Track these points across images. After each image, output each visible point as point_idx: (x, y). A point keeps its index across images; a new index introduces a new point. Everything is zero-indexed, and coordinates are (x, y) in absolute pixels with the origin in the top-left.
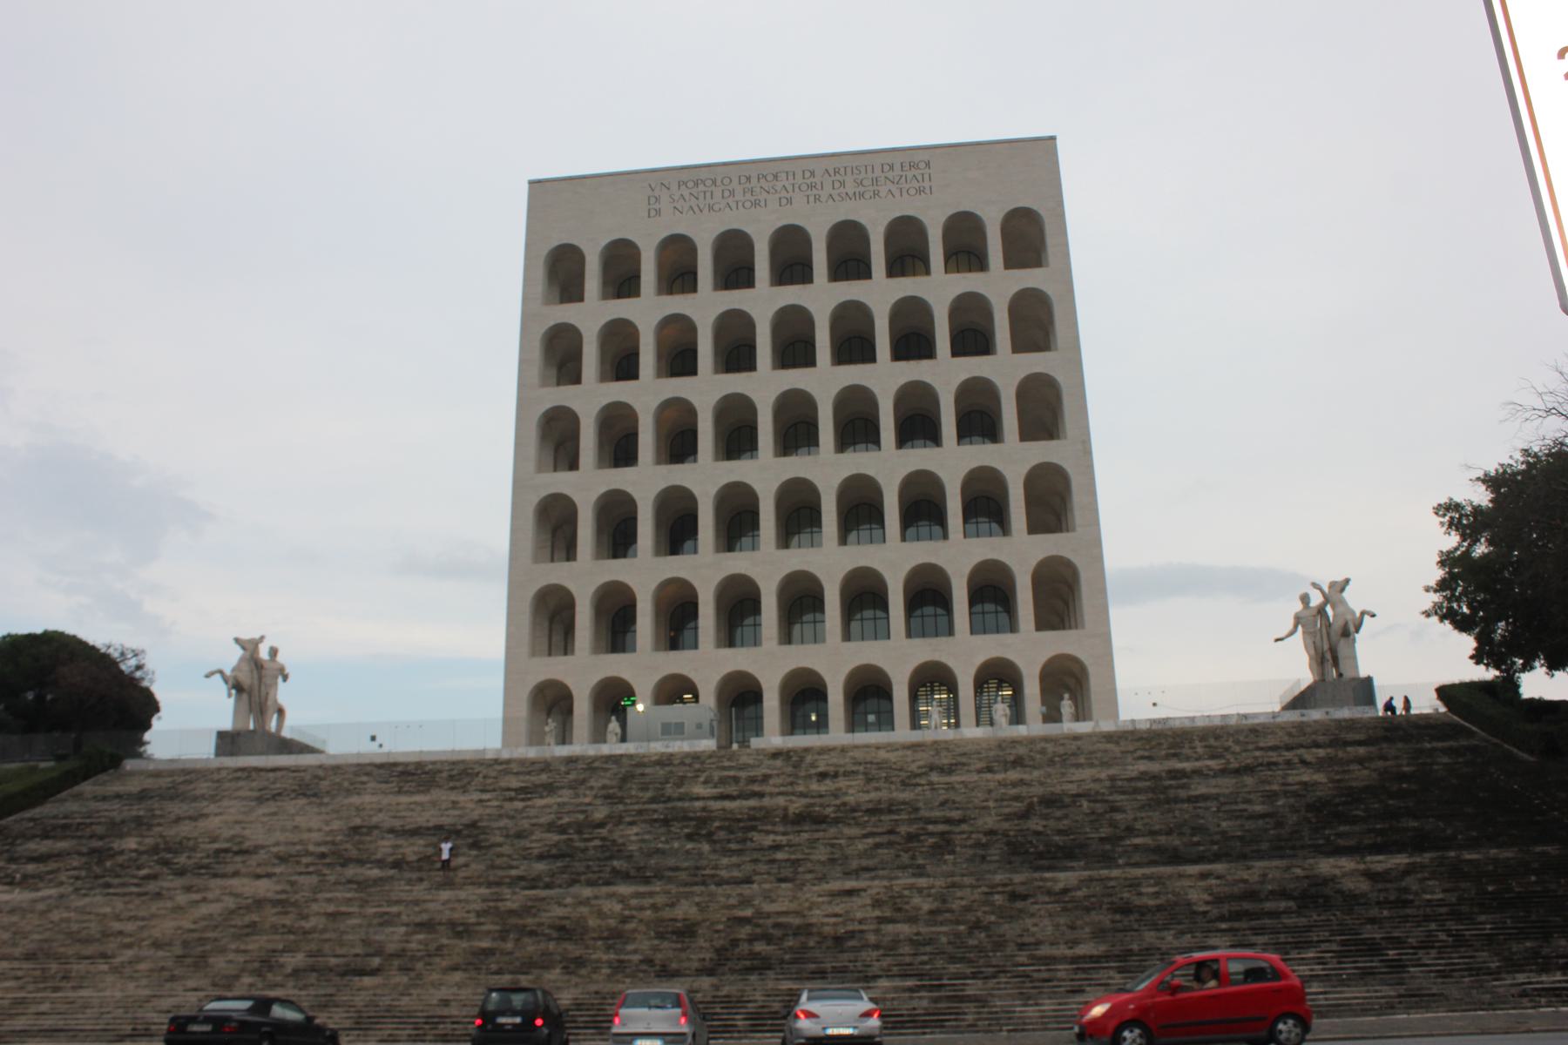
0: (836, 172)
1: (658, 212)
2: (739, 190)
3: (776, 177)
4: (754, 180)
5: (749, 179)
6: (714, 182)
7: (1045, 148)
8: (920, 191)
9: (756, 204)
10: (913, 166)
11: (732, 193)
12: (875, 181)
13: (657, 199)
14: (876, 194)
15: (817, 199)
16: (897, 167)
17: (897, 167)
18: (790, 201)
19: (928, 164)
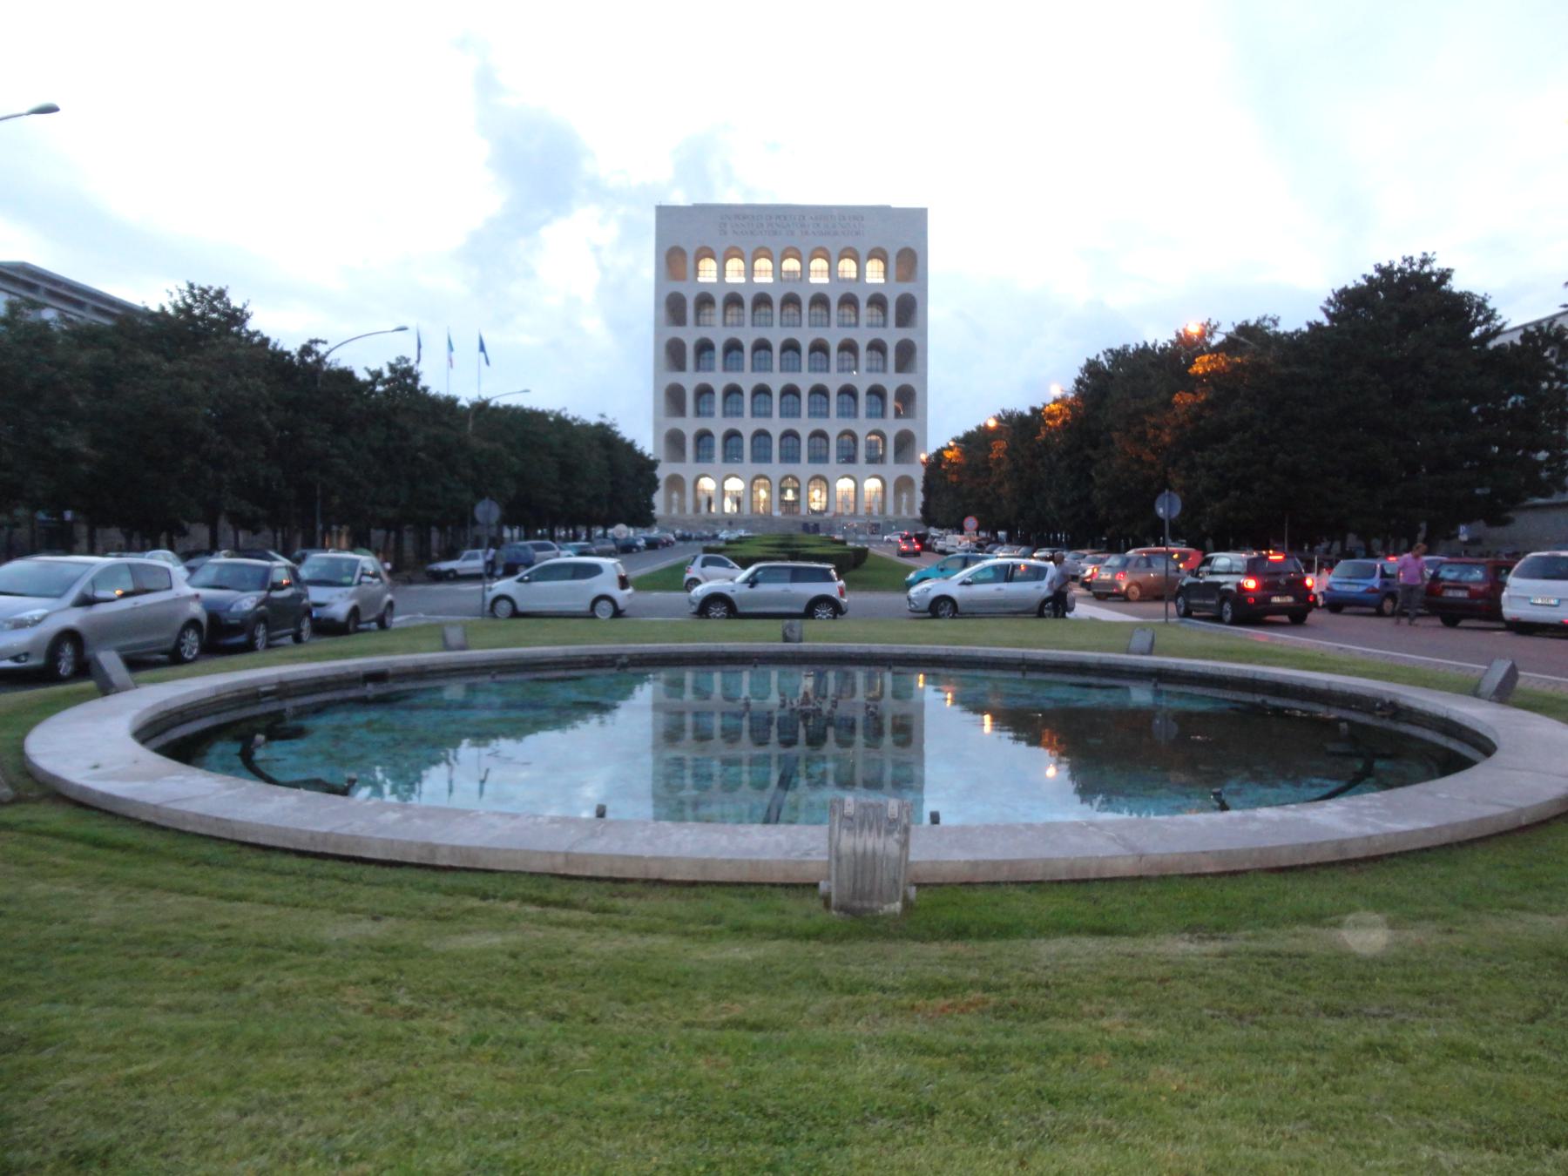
1: (725, 233)
8: (857, 233)
9: (775, 233)
10: (855, 218)
12: (834, 226)
13: (725, 225)
15: (807, 233)
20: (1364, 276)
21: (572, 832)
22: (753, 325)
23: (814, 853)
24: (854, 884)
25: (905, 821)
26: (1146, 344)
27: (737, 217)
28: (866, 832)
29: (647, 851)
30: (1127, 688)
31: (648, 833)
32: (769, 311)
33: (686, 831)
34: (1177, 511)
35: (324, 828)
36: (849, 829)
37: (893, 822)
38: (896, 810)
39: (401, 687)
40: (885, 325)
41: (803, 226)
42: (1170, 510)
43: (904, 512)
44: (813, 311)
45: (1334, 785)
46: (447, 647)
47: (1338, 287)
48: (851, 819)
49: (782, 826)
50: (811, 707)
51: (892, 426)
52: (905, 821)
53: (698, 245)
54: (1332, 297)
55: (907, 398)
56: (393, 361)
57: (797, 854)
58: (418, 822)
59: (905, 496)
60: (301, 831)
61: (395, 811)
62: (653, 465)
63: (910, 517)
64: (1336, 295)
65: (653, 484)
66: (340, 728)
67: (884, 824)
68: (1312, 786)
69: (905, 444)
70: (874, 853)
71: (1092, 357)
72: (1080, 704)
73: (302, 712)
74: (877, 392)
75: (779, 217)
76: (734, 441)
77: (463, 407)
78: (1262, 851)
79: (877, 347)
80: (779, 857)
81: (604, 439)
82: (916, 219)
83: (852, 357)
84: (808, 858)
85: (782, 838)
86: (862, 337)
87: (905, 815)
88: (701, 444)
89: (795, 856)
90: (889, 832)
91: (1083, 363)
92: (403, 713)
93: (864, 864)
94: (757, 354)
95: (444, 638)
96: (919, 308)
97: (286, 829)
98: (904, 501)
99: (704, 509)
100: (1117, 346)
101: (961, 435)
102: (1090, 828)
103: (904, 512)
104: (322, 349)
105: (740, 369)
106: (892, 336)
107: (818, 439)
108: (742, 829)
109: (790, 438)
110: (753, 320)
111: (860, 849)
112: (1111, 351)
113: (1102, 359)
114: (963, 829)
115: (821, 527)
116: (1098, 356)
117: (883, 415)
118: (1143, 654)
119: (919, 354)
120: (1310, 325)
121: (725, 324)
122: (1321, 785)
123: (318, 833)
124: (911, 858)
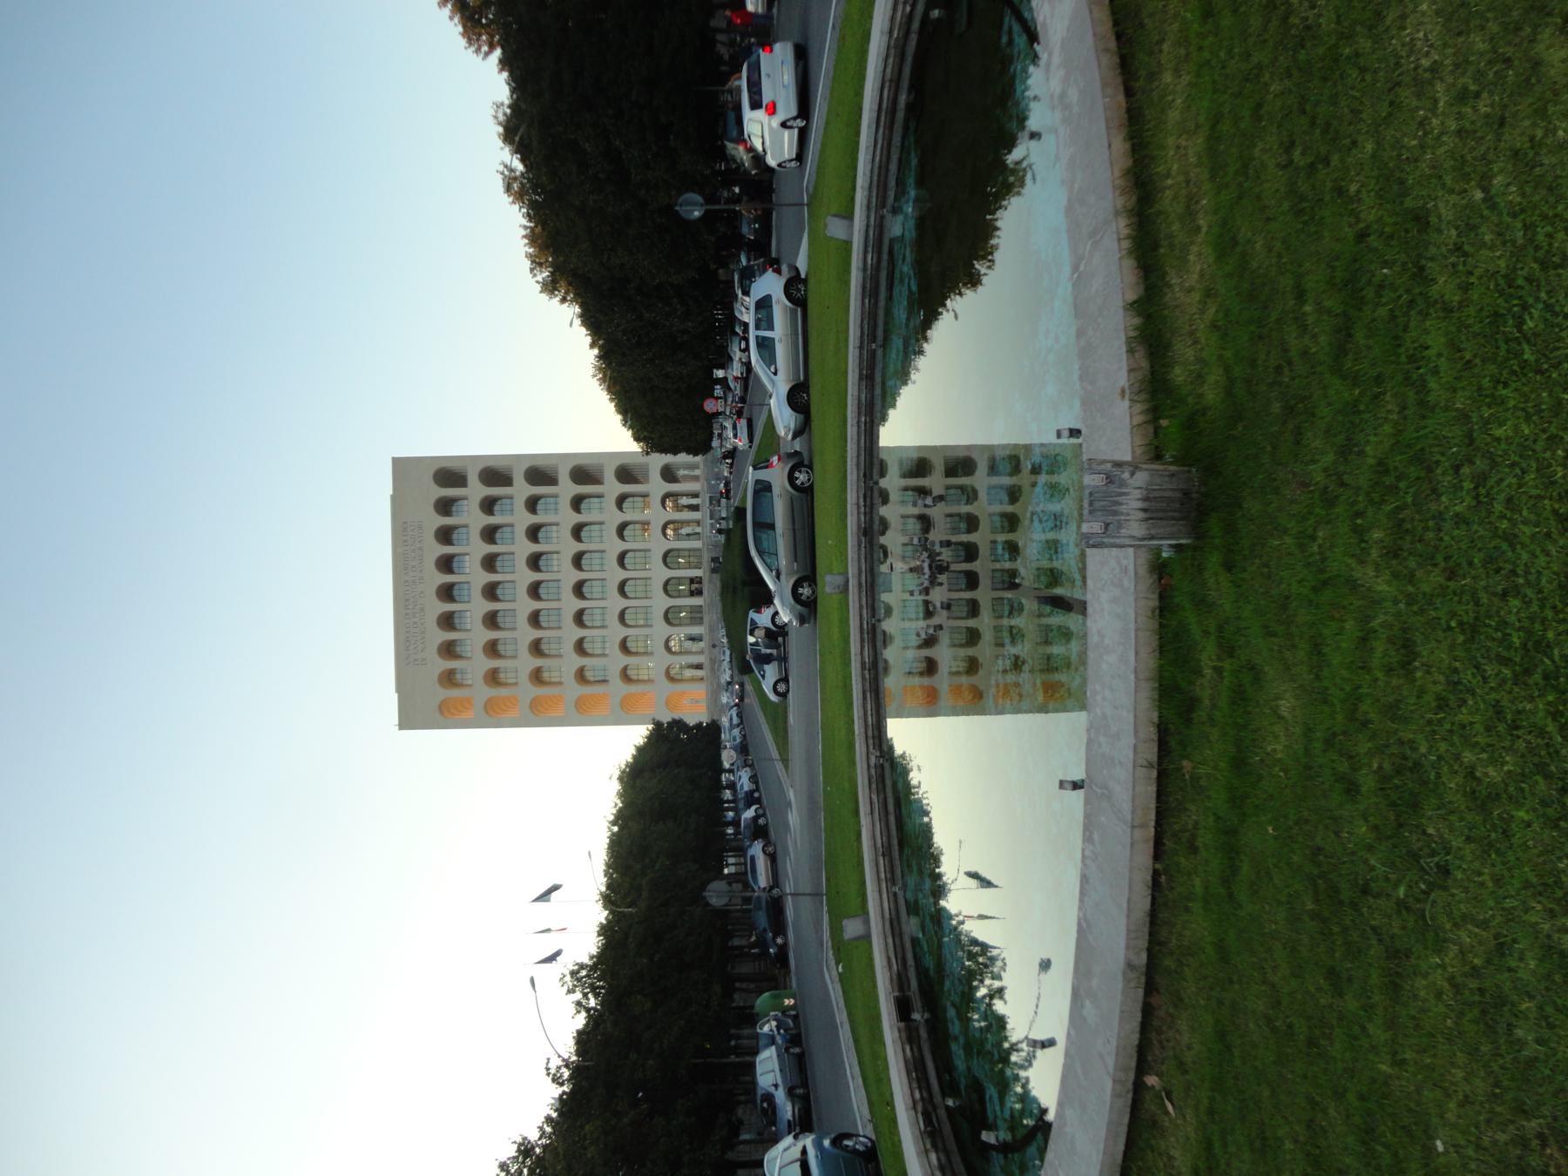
0: (406, 569)
1: (424, 660)
2: (415, 620)
3: (407, 600)
4: (408, 611)
6: (407, 632)
7: (402, 468)
8: (420, 527)
9: (422, 610)
10: (405, 530)
11: (415, 623)
13: (416, 660)
14: (420, 549)
15: (421, 578)
16: (405, 538)
17: (405, 538)
18: (422, 592)
20: (451, 18)
21: (1103, 819)
22: (514, 629)
23: (1124, 562)
24: (1173, 519)
25: (1109, 466)
26: (525, 237)
28: (1123, 508)
29: (1128, 740)
30: (892, 241)
31: (1102, 739)
33: (1099, 698)
34: (699, 198)
35: (1109, 1085)
36: (1120, 526)
37: (1110, 479)
38: (1093, 476)
39: (914, 983)
40: (511, 498)
41: (414, 582)
42: (694, 204)
43: (697, 472)
44: (499, 569)
45: (1008, 20)
46: (866, 937)
47: (463, 42)
48: (1107, 525)
49: (1089, 597)
50: (926, 565)
51: (613, 487)
52: (1109, 466)
54: (473, 49)
55: (585, 473)
56: (565, 989)
57: (1126, 583)
58: (1094, 983)
60: (1111, 1107)
61: (1082, 1006)
62: (658, 725)
63: (701, 466)
64: (470, 44)
65: (678, 724)
66: (968, 1048)
67: (1112, 488)
68: (1011, 42)
69: (626, 474)
70: (1146, 499)
71: (539, 287)
72: (914, 288)
73: (950, 1088)
76: (630, 645)
77: (606, 919)
78: (1104, 85)
79: (532, 504)
80: (1132, 598)
81: (636, 777)
82: (402, 468)
83: (543, 529)
84: (1131, 567)
85: (1104, 597)
86: (524, 519)
87: (1103, 467)
88: (635, 678)
89: (1129, 583)
90: (1123, 484)
91: (544, 297)
92: (947, 984)
93: (1155, 510)
94: (543, 624)
95: (858, 938)
96: (490, 464)
97: (1110, 1123)
98: (686, 472)
99: (699, 673)
100: (527, 264)
101: (619, 417)
102: (1082, 268)
103: (697, 472)
104: (555, 1062)
105: (559, 640)
106: (522, 490)
107: (626, 561)
108: (1093, 639)
109: (627, 589)
110: (509, 629)
111: (1141, 515)
112: (532, 270)
113: (539, 278)
114: (1086, 403)
115: (714, 555)
116: (538, 282)
118: (851, 226)
119: (539, 463)
120: (501, 70)
121: (514, 657)
122: (1010, 32)
123: (1113, 1090)
124: (1128, 458)
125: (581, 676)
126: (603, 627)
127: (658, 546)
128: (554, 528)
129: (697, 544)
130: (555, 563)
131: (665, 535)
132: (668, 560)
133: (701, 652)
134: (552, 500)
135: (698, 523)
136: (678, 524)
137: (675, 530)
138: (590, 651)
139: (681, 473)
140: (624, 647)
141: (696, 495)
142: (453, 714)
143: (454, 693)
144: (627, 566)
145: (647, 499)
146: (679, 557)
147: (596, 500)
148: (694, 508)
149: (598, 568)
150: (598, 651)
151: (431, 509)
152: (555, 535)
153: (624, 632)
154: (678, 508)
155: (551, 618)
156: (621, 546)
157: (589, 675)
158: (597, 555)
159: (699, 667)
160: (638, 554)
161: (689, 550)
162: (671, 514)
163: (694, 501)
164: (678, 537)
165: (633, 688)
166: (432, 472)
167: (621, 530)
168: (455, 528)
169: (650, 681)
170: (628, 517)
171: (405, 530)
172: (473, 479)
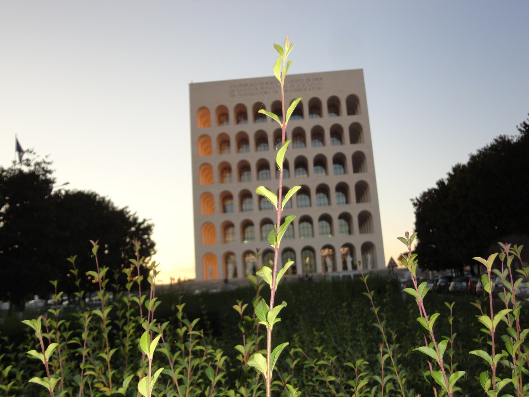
1: (234, 96)
3: (272, 83)
5: (263, 84)
8: (319, 88)
9: (266, 93)
10: (317, 79)
11: (257, 89)
19: (321, 79)
27: (241, 85)
32: (266, 145)
53: (217, 105)
59: (369, 257)
74: (342, 188)
75: (267, 83)
76: (249, 229)
79: (339, 160)
96: (364, 129)
99: (230, 276)
105: (249, 180)
117: (347, 202)
125: (227, 196)
126: (260, 209)
127: (317, 243)
128: (324, 174)
129: (320, 269)
130: (302, 176)
131: (325, 247)
132: (308, 252)
133: (245, 275)
134: (342, 171)
135: (334, 269)
136: (333, 257)
137: (329, 255)
138: (244, 202)
139: (369, 257)
140: (247, 224)
141: (354, 267)
142: (201, 118)
143: (213, 117)
144: (302, 225)
145: (348, 233)
146: (310, 257)
147: (344, 200)
148: (345, 268)
149: (300, 204)
150: (244, 207)
151: (331, 94)
152: (320, 174)
153: (257, 221)
154: (344, 256)
155: (264, 176)
156: (315, 219)
157: (229, 202)
158: (308, 202)
159: (235, 275)
160: (310, 230)
161: (315, 264)
162: (340, 251)
163: (349, 266)
164: (324, 257)
165: (218, 230)
166: (356, 93)
167: (326, 218)
168: (320, 114)
169: (225, 242)
170: (336, 222)
171: (317, 79)
172: (353, 119)
